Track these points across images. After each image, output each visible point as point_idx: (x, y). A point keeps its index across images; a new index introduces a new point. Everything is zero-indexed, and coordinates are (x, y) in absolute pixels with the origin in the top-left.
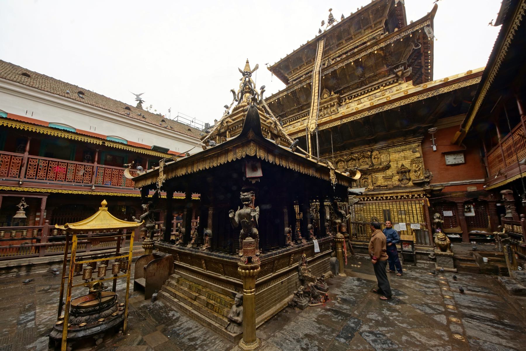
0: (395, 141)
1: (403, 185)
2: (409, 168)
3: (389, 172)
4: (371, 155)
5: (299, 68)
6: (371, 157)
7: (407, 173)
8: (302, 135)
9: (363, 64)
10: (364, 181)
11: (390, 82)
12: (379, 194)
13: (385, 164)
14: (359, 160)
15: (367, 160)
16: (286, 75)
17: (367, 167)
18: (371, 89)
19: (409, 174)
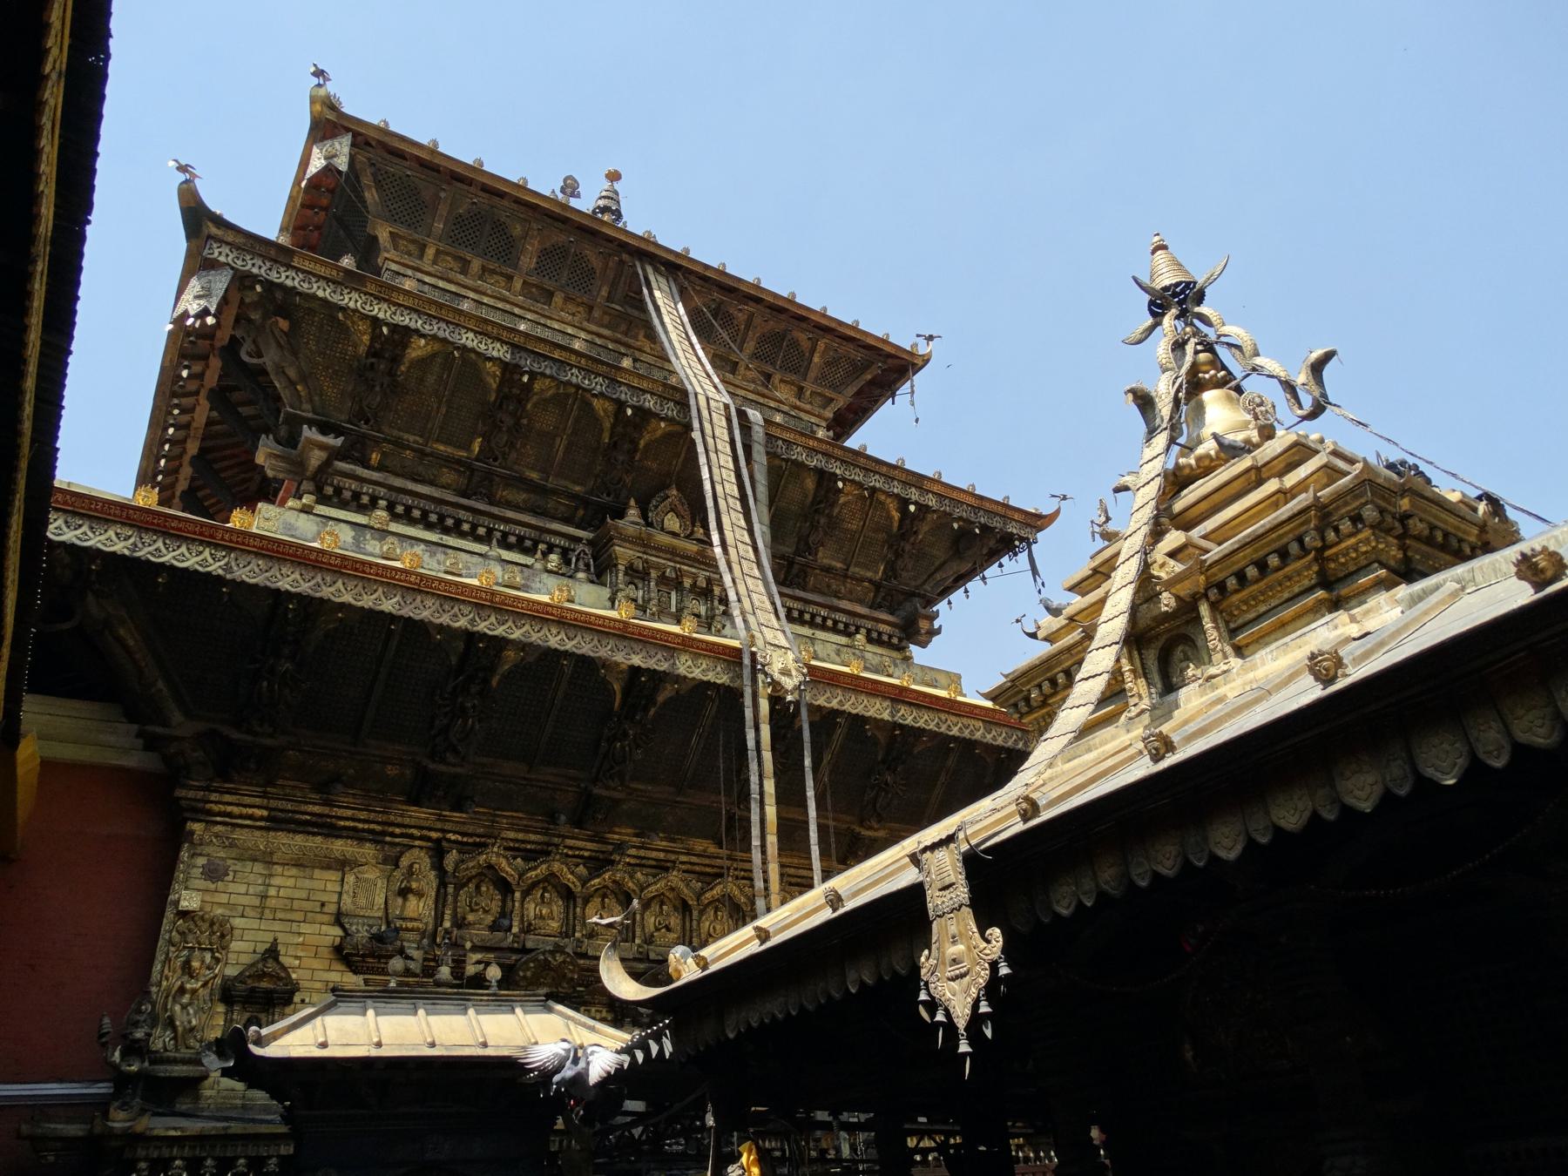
5: (476, 264)
8: (697, 674)
9: (836, 511)
11: (880, 634)
16: (383, 234)
18: (825, 619)
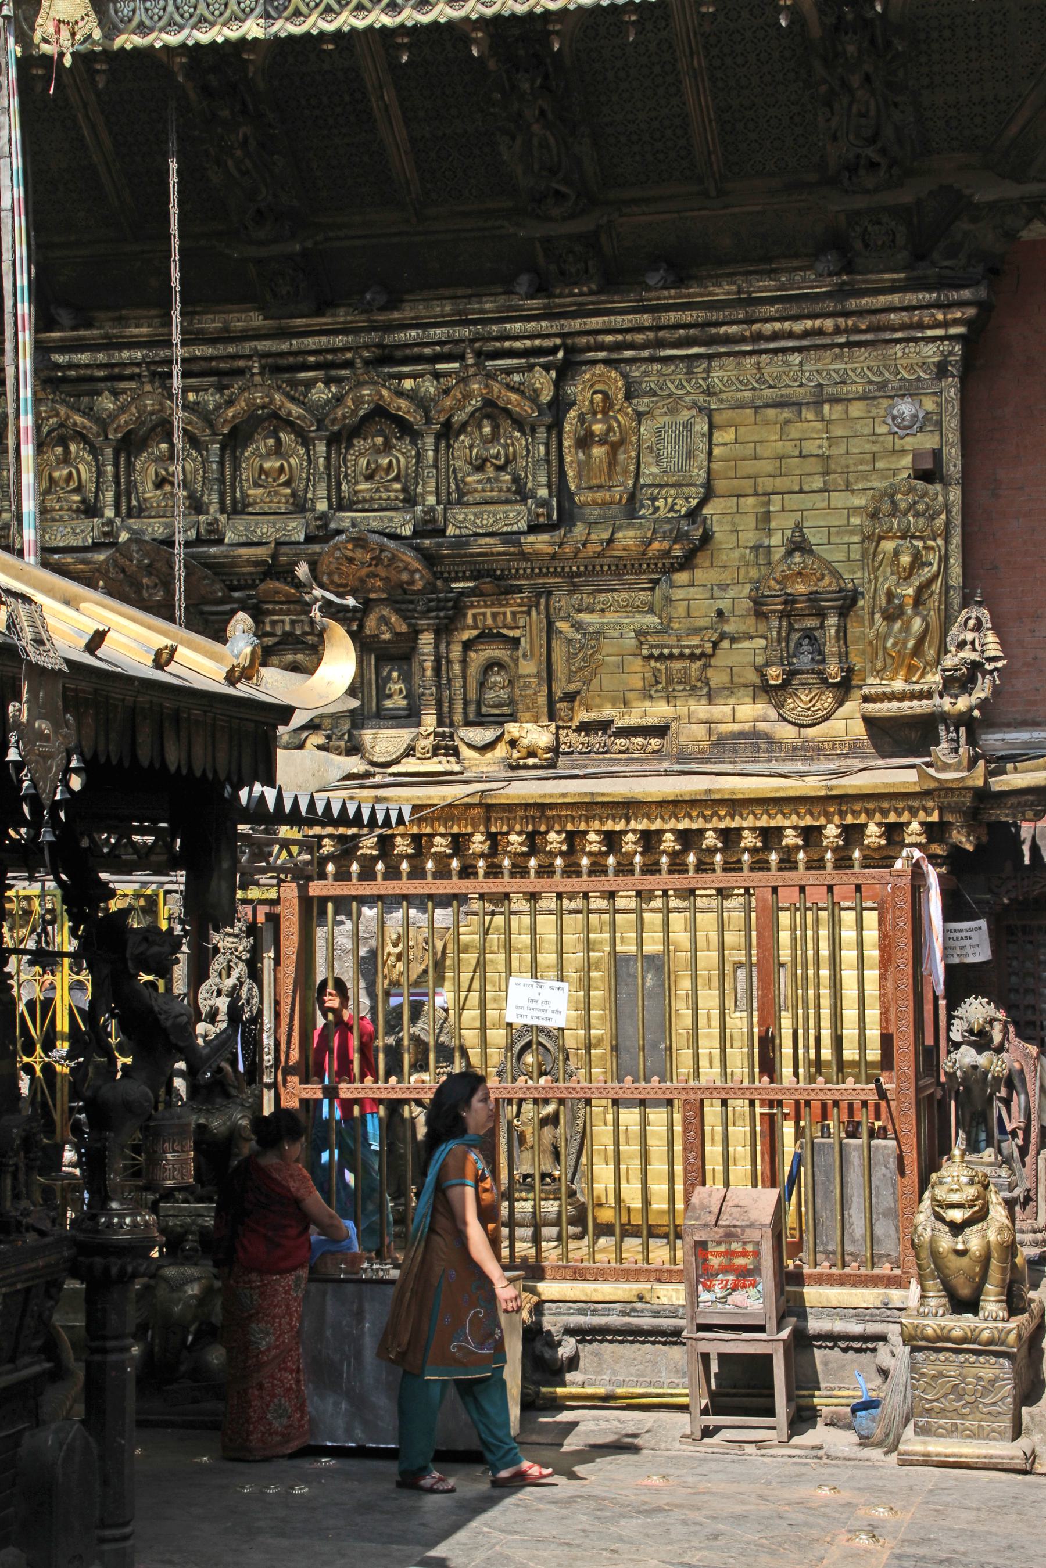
0: (763, 287)
1: (786, 732)
2: (853, 576)
3: (693, 595)
4: (559, 405)
6: (556, 427)
7: (832, 621)
10: (478, 658)
12: (593, 808)
13: (670, 504)
14: (447, 433)
15: (519, 441)
17: (515, 518)
19: (842, 632)
